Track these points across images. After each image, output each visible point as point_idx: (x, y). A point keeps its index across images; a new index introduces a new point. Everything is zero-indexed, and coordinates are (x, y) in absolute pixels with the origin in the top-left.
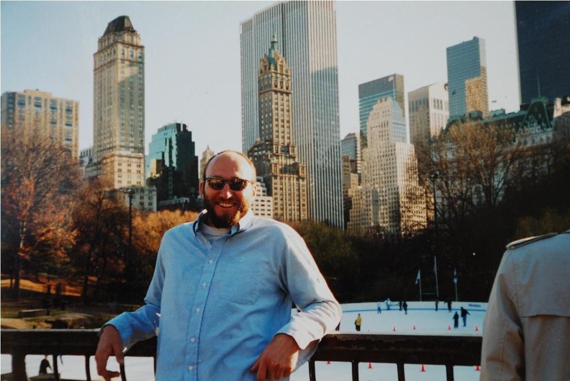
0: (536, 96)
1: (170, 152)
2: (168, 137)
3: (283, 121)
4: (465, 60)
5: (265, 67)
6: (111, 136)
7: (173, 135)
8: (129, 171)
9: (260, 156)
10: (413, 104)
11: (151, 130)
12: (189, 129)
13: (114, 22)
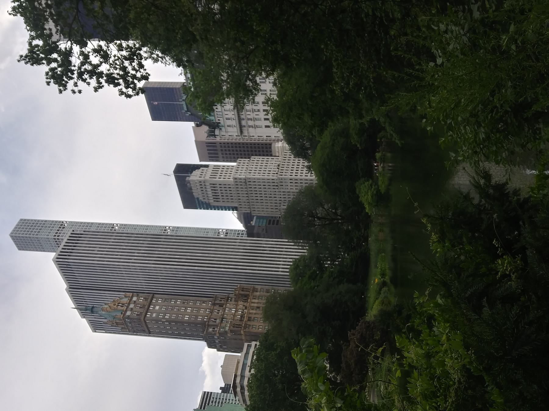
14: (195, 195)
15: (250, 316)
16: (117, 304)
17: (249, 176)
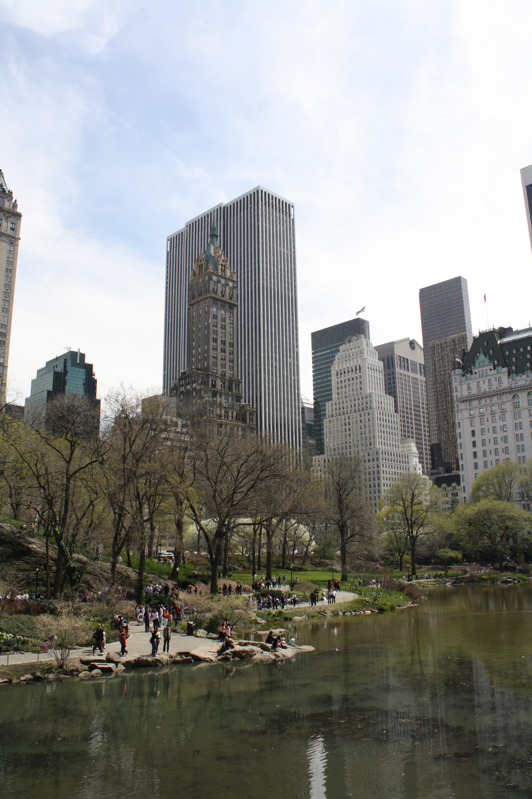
3: (223, 343)
5: (200, 266)
9: (188, 392)
14: (341, 348)
15: (223, 427)
16: (224, 263)
17: (376, 412)
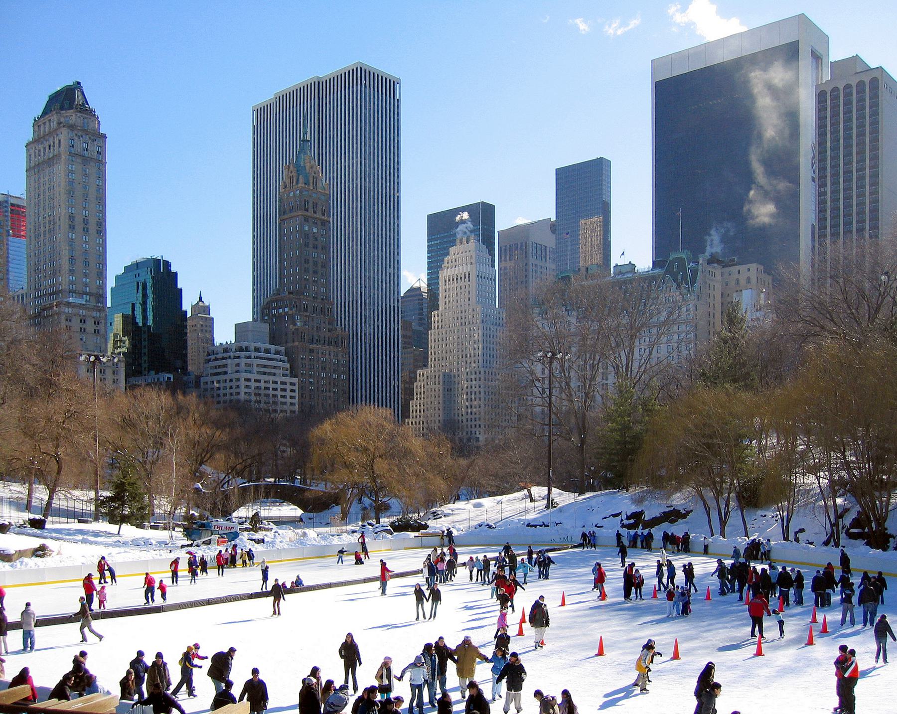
0: (677, 250)
1: (144, 303)
2: (141, 279)
4: (583, 187)
6: (54, 274)
7: (147, 277)
8: (83, 330)
10: (505, 250)
11: (115, 268)
12: (173, 269)
13: (58, 94)
